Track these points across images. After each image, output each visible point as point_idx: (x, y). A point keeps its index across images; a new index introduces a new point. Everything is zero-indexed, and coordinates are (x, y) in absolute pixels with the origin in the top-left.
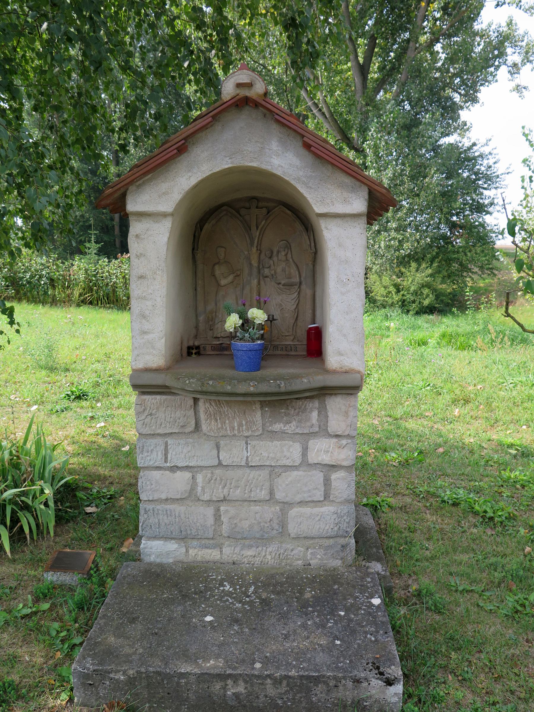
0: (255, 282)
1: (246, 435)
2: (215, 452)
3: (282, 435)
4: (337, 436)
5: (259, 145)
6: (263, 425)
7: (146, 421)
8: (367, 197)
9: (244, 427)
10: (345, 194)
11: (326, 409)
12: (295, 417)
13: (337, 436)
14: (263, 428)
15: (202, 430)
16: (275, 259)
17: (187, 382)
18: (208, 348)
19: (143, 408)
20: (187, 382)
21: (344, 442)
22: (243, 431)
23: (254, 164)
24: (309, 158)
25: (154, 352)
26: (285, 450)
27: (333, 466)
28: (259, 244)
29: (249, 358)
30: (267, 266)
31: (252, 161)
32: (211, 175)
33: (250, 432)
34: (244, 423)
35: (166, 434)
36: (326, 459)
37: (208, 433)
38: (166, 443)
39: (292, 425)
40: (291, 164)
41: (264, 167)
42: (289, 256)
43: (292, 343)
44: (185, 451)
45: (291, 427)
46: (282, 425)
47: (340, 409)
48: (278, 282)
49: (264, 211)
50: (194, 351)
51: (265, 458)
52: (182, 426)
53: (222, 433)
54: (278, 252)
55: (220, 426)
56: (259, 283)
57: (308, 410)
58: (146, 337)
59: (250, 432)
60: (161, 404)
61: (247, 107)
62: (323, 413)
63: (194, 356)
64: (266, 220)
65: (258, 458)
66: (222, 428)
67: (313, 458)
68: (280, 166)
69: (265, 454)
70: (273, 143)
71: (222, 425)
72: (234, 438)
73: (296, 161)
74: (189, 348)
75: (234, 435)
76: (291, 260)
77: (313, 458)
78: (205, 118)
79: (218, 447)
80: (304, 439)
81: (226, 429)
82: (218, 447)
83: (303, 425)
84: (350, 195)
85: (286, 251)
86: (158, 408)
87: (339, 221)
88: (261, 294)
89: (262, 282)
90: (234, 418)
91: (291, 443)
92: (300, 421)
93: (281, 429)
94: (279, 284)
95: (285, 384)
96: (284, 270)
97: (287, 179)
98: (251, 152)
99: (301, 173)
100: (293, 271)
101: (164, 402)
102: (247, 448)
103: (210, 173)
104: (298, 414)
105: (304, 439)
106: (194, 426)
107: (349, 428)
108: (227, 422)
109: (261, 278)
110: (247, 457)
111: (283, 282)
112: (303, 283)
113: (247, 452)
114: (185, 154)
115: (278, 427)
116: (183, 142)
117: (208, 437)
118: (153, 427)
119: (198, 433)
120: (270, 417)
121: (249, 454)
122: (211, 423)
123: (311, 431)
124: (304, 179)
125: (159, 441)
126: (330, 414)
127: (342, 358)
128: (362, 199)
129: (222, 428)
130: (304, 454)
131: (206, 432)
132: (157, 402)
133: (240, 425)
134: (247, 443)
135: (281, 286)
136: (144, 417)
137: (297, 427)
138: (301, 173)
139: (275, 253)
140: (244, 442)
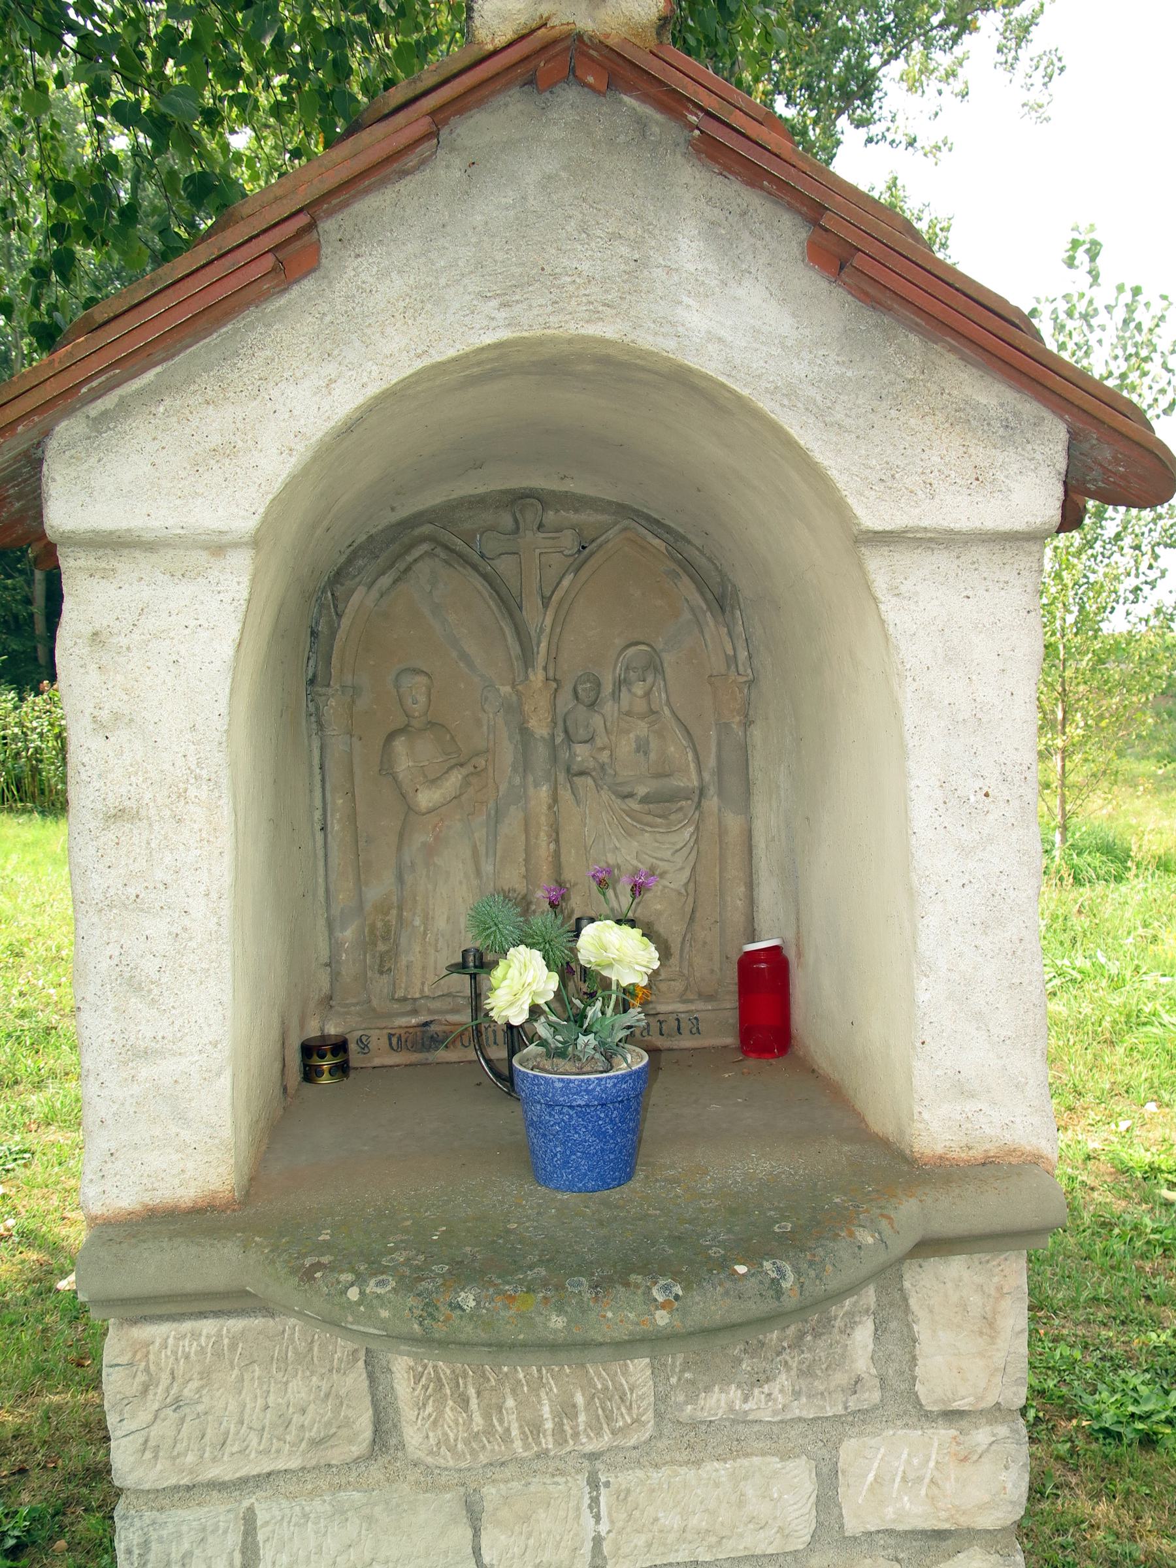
0: (544, 791)
1: (589, 1448)
2: (462, 1534)
3: (734, 1438)
4: (952, 1416)
5: (624, 250)
6: (661, 1399)
7: (155, 1431)
8: (1062, 464)
9: (582, 1418)
10: (980, 454)
11: (907, 1309)
12: (785, 1356)
13: (952, 1416)
14: (659, 1416)
15: (401, 1446)
16: (609, 708)
17: (353, 1294)
18: (378, 1040)
19: (141, 1378)
20: (353, 1294)
21: (982, 1436)
22: (576, 1435)
23: (608, 330)
24: (831, 304)
25: (186, 1134)
26: (750, 1492)
27: (939, 1535)
28: (554, 657)
29: (601, 1134)
30: (582, 733)
31: (595, 317)
32: (418, 377)
33: (607, 1437)
34: (579, 1399)
35: (244, 1481)
36: (912, 1510)
37: (430, 1460)
38: (249, 1522)
39: (774, 1388)
40: (756, 331)
41: (648, 340)
42: (659, 697)
43: (681, 1007)
44: (331, 1544)
45: (776, 1398)
46: (734, 1393)
47: (963, 1306)
48: (626, 789)
49: (568, 541)
50: (326, 1064)
51: (671, 1538)
52: (316, 1443)
53: (496, 1448)
54: (620, 684)
55: (478, 1422)
56: (555, 799)
57: (838, 1323)
58: (145, 1071)
59: (607, 1437)
60: (218, 1355)
61: (570, 95)
62: (893, 1325)
63: (325, 1080)
64: (577, 571)
65: (641, 1540)
66: (489, 1431)
67: (859, 1513)
68: (711, 337)
69: (671, 1520)
70: (683, 243)
71: (487, 1417)
72: (538, 1465)
73: (779, 320)
74: (309, 1050)
75: (543, 1455)
76: (667, 711)
77: (859, 1513)
78: (400, 118)
79: (474, 1515)
80: (821, 1441)
81: (506, 1438)
82: (474, 1515)
83: (819, 1386)
84: (1000, 457)
85: (650, 680)
86: (206, 1375)
87: (942, 560)
88: (562, 837)
89: (565, 794)
90: (537, 1385)
91: (775, 1462)
92: (807, 1372)
93: (731, 1409)
94: (631, 795)
95: (798, 1272)
96: (642, 747)
97: (745, 392)
98: (590, 279)
99: (800, 369)
100: (676, 749)
101: (233, 1347)
102: (595, 1501)
103: (418, 365)
104: (797, 1343)
105: (821, 1441)
106: (368, 1434)
107: (997, 1379)
108: (510, 1403)
109: (562, 777)
110: (598, 1541)
111: (642, 791)
112: (712, 790)
113: (598, 1521)
114: (308, 285)
115: (719, 1402)
116: (303, 220)
117: (430, 1479)
118: (190, 1458)
119: (383, 1460)
120: (686, 1366)
121: (603, 1528)
122: (441, 1413)
123: (852, 1405)
124: (812, 392)
125: (221, 1514)
126: (921, 1329)
127: (970, 1106)
128: (1044, 471)
129: (489, 1431)
130: (827, 1500)
131: (420, 1454)
132: (202, 1351)
133: (567, 1410)
134: (594, 1483)
135: (634, 805)
136: (144, 1417)
137: (797, 1394)
138: (800, 369)
139: (607, 688)
140: (582, 1479)
